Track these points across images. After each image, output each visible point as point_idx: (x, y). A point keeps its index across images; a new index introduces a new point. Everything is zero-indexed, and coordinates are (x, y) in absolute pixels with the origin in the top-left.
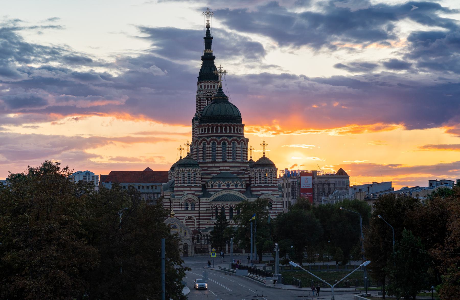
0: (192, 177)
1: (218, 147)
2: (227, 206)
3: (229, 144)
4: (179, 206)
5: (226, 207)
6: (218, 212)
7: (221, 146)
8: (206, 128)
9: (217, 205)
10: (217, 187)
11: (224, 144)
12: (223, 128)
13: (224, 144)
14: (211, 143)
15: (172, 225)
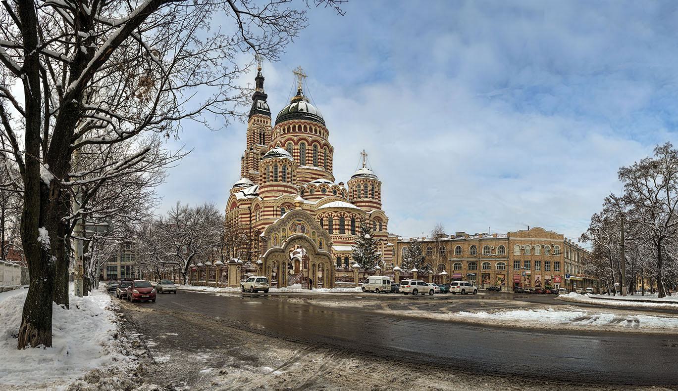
0: (288, 174)
1: (310, 149)
2: (349, 215)
3: (322, 148)
4: (272, 213)
5: (347, 217)
6: (334, 223)
7: (312, 148)
8: (291, 126)
9: (332, 213)
10: (321, 193)
11: (315, 147)
12: (312, 129)
13: (315, 146)
14: (299, 144)
15: (298, 224)
